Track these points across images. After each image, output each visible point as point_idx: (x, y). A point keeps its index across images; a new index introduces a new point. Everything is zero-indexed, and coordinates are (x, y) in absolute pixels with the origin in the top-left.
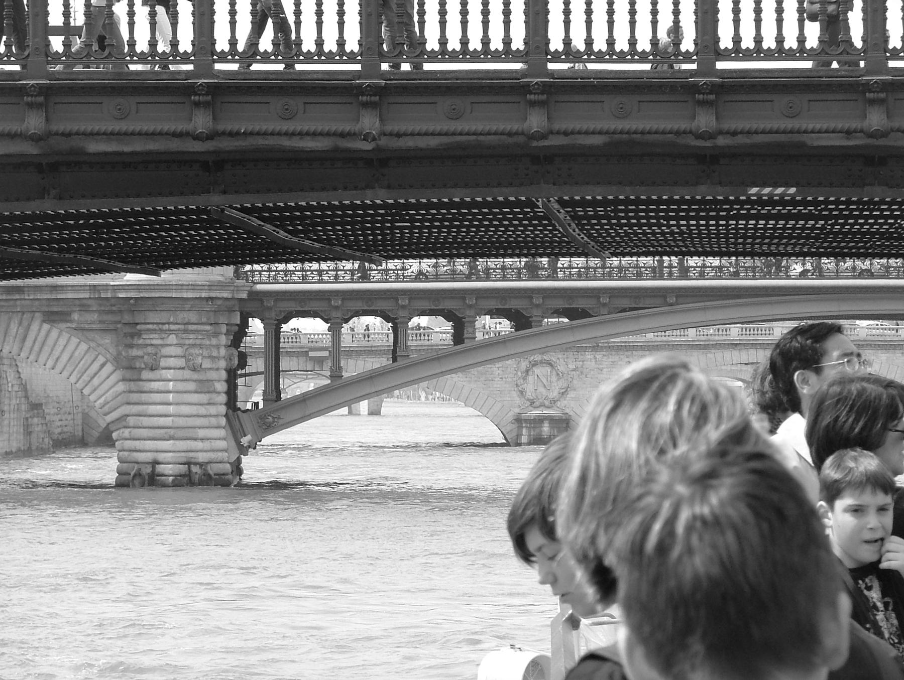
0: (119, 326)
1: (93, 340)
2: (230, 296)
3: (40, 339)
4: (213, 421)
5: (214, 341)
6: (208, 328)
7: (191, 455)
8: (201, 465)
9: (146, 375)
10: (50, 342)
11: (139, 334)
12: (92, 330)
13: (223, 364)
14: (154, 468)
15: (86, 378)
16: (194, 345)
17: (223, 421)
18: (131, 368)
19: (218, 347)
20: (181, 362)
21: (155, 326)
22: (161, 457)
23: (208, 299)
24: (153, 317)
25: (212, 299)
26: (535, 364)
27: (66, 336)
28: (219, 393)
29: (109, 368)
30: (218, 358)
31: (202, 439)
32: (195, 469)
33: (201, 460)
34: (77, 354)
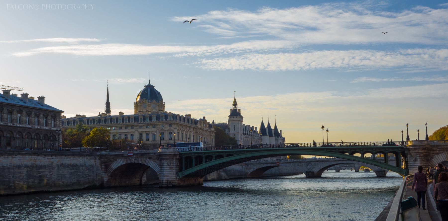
1: (156, 162)
2: (174, 154)
3: (148, 162)
5: (173, 161)
8: (169, 181)
9: (162, 167)
10: (149, 162)
15: (154, 167)
16: (169, 162)
17: (175, 174)
18: (161, 166)
19: (174, 162)
20: (167, 165)
24: (162, 158)
25: (171, 154)
26: (309, 164)
28: (174, 169)
29: (158, 166)
30: (174, 164)
31: (170, 177)
32: (169, 182)
33: (170, 180)
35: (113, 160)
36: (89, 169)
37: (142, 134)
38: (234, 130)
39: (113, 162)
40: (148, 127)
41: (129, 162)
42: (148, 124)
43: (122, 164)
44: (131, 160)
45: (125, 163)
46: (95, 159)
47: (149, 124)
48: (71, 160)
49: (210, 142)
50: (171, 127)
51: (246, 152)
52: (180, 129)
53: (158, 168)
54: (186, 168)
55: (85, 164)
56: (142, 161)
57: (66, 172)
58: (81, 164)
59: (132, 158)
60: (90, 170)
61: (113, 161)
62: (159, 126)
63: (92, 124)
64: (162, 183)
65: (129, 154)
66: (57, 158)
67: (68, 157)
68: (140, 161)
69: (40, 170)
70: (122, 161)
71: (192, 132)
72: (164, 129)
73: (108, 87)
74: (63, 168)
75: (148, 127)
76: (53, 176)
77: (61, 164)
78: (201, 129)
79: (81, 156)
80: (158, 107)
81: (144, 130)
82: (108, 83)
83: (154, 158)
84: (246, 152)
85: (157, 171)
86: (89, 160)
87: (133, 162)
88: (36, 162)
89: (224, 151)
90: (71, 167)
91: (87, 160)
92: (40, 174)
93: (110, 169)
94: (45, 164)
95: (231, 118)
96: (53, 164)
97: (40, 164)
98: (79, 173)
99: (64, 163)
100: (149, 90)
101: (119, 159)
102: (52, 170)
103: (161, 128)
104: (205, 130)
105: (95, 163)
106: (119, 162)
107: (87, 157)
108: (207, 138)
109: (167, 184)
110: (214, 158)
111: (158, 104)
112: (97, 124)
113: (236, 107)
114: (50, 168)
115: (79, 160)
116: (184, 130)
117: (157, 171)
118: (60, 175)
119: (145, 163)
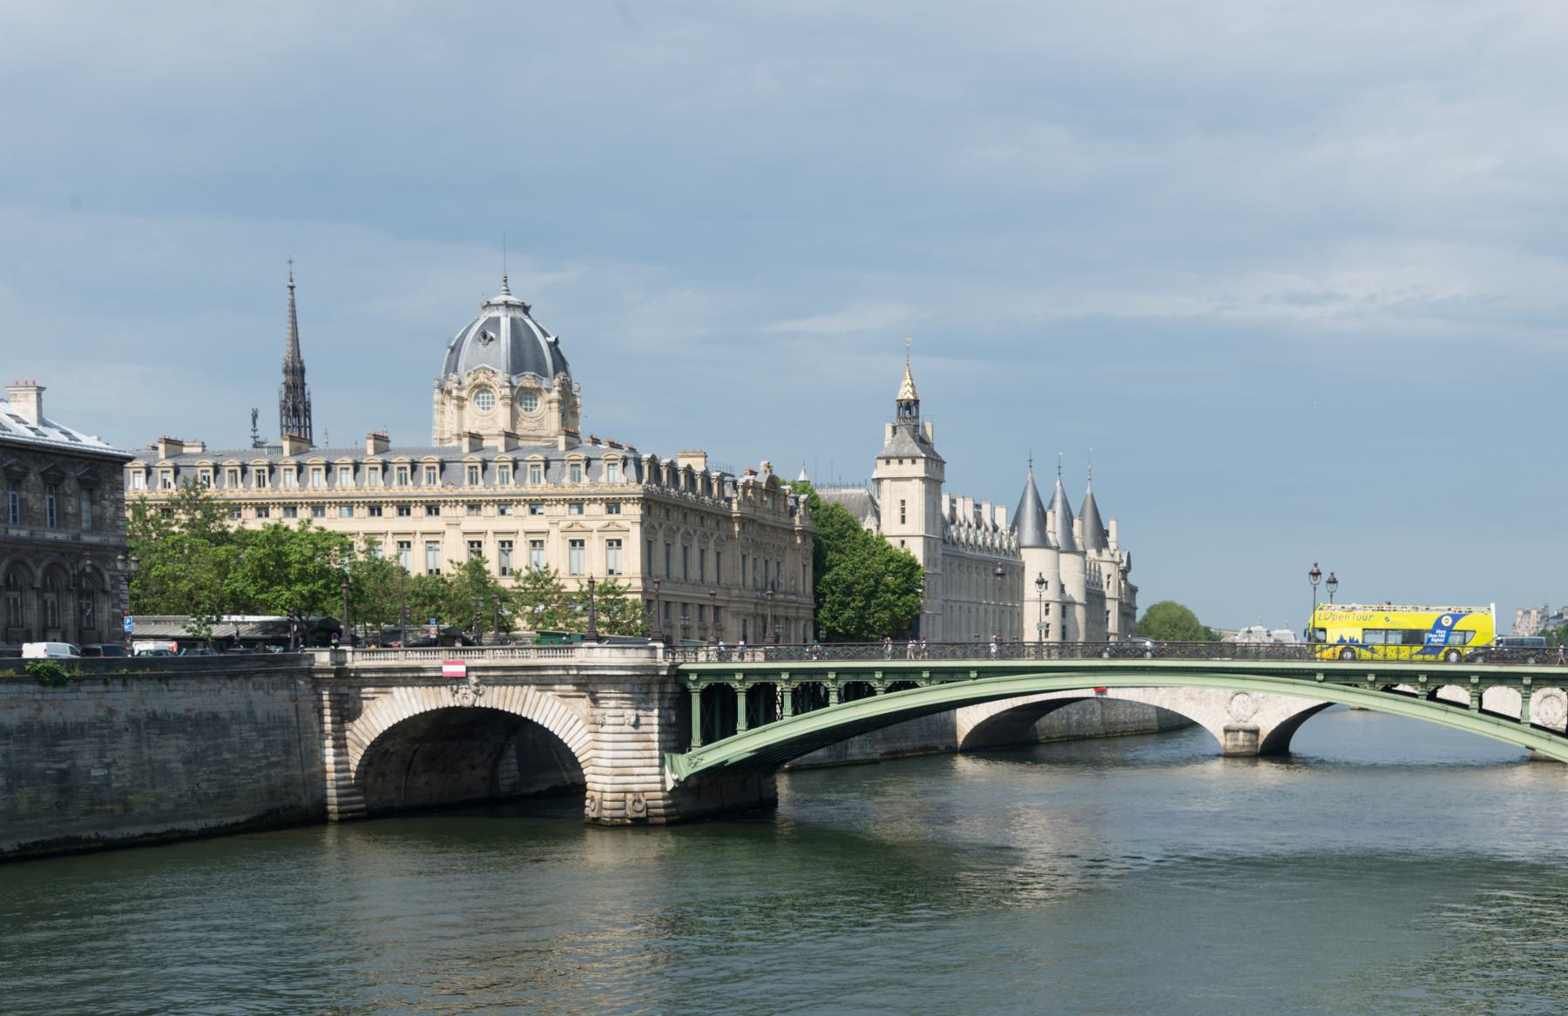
1: (570, 704)
4: (648, 762)
5: (651, 705)
6: (642, 696)
13: (656, 720)
15: (565, 730)
20: (620, 720)
28: (653, 741)
31: (638, 775)
33: (636, 790)
36: (269, 736)
37: (479, 544)
38: (903, 520)
39: (374, 698)
40: (508, 511)
41: (443, 698)
42: (508, 498)
43: (417, 713)
44: (459, 696)
45: (428, 709)
46: (293, 686)
47: (514, 498)
48: (191, 694)
49: (793, 582)
50: (618, 512)
51: (974, 675)
52: (660, 526)
53: (581, 734)
54: (708, 738)
55: (251, 713)
56: (508, 700)
57: (171, 750)
58: (232, 712)
60: (271, 738)
61: (376, 695)
62: (562, 509)
63: (240, 485)
64: (602, 800)
66: (131, 691)
67: (176, 685)
69: (59, 745)
71: (715, 538)
72: (581, 522)
73: (292, 288)
74: (157, 731)
75: (508, 511)
76: (118, 773)
77: (148, 714)
78: (754, 521)
79: (232, 676)
80: (550, 408)
81: (488, 522)
82: (293, 265)
83: (564, 687)
84: (974, 675)
86: (269, 694)
87: (467, 703)
88: (40, 710)
89: (879, 669)
90: (192, 726)
91: (260, 693)
92: (60, 762)
93: (359, 734)
94: (80, 720)
95: (888, 462)
96: (115, 718)
97: (60, 720)
98: (227, 755)
99: (159, 711)
100: (505, 324)
101: (402, 689)
102: (110, 746)
103: (569, 517)
104: (773, 524)
105: (291, 706)
107: (259, 679)
108: (779, 563)
110: (833, 698)
111: (547, 397)
112: (263, 489)
113: (910, 413)
114: (101, 736)
115: (225, 692)
116: (675, 528)
118: (147, 767)
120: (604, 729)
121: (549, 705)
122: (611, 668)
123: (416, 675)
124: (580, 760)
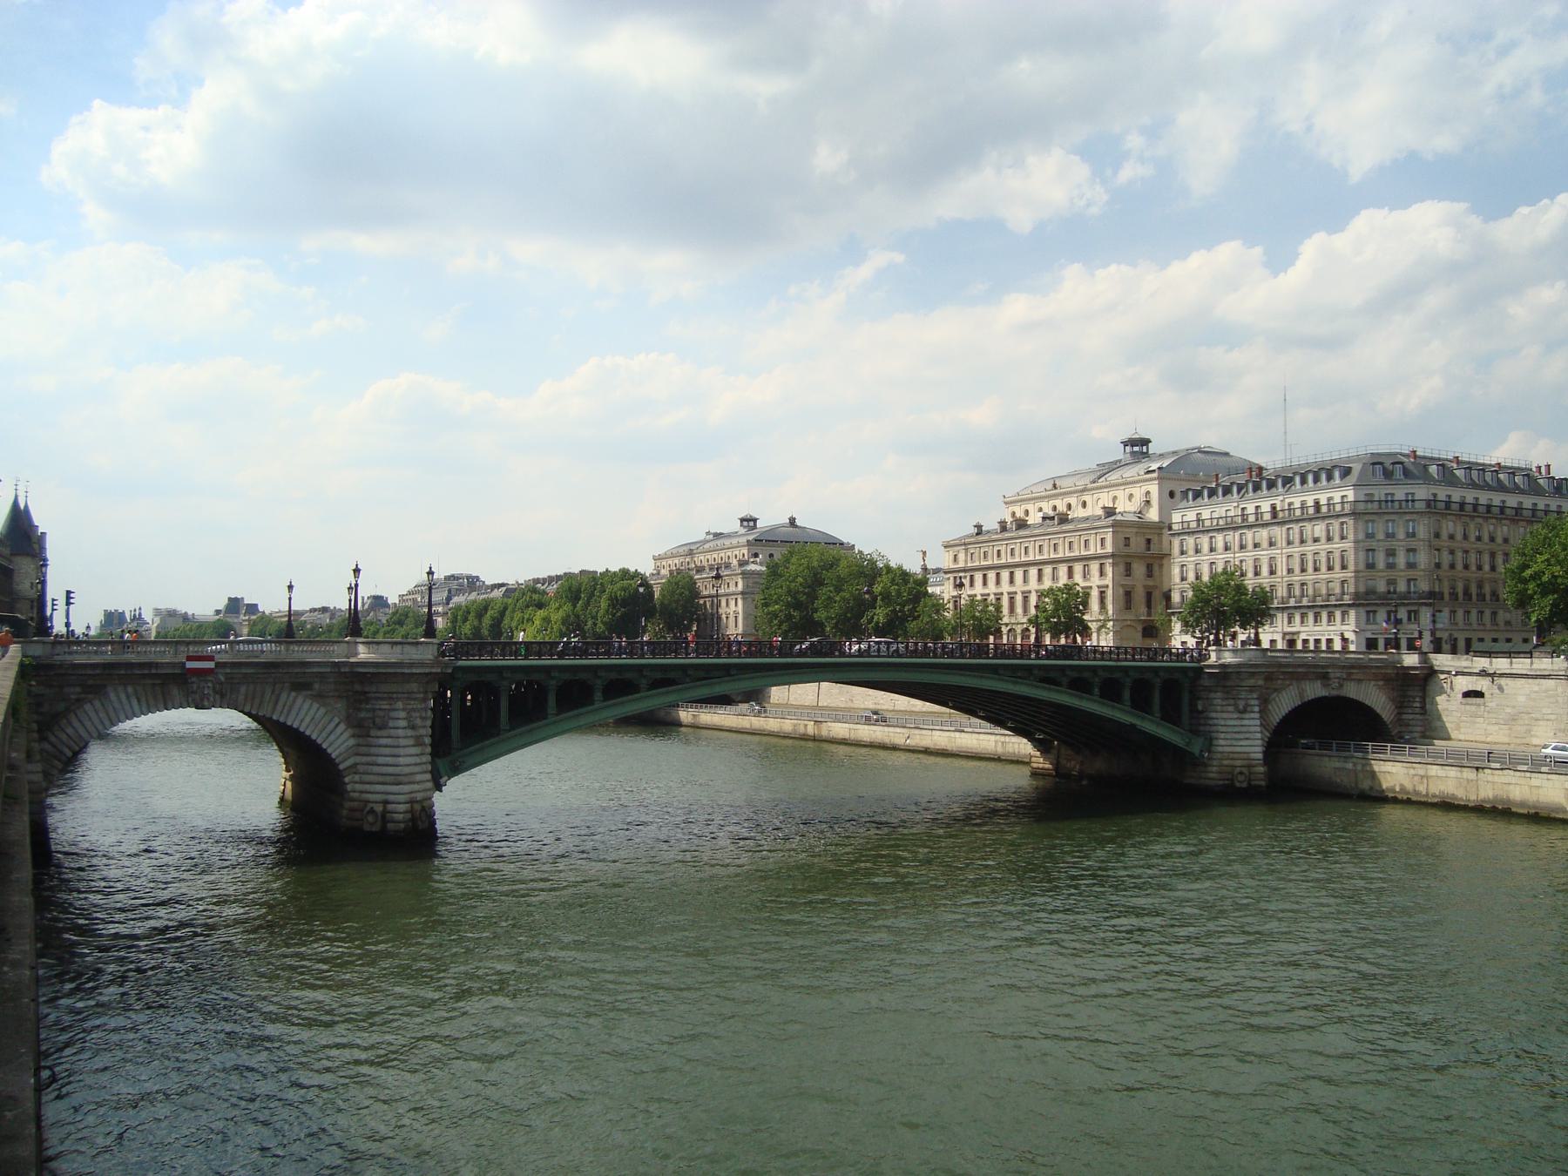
0: (350, 693)
7: (413, 795)
9: (373, 732)
11: (367, 701)
12: (328, 697)
14: (385, 808)
15: (324, 735)
21: (386, 695)
22: (391, 798)
23: (427, 674)
24: (384, 688)
27: (309, 702)
29: (342, 726)
32: (417, 807)
34: (317, 715)
35: (80, 693)
56: (257, 701)
59: (202, 684)
61: (83, 696)
64: (385, 812)
65: (190, 665)
68: (246, 699)
70: (139, 701)
85: (337, 753)
101: (120, 689)
106: (117, 705)
109: (409, 816)
110: (598, 695)
117: (340, 754)
119: (273, 713)
120: (383, 733)
121: (306, 706)
122: (411, 665)
123: (146, 672)
124: (341, 767)
